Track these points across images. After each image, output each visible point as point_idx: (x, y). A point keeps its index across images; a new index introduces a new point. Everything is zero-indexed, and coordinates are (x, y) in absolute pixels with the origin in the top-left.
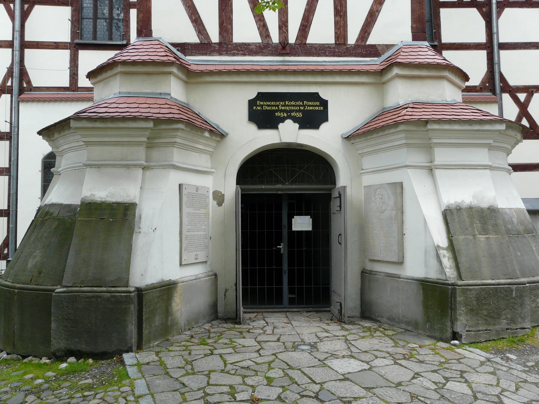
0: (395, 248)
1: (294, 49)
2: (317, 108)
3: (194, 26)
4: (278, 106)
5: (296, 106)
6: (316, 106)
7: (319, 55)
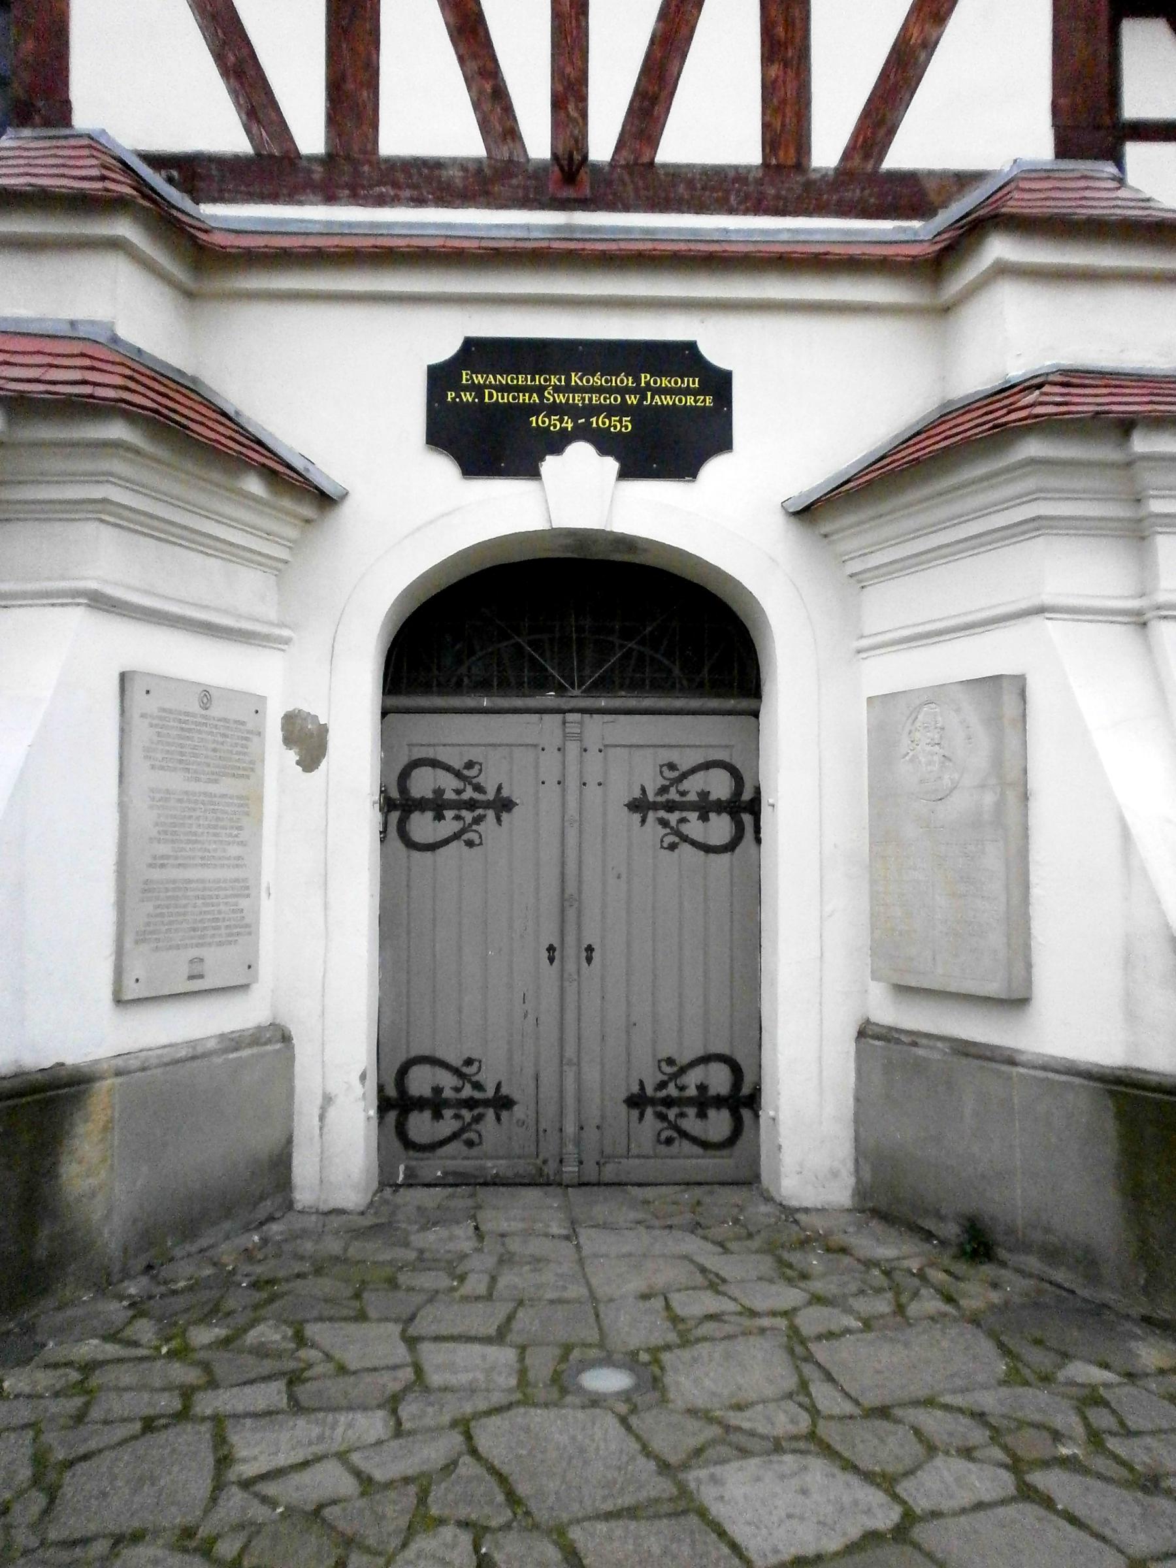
0: (996, 939)
1: (609, 183)
2: (690, 401)
3: (234, 93)
4: (540, 390)
5: (610, 391)
6: (688, 391)
7: (700, 207)
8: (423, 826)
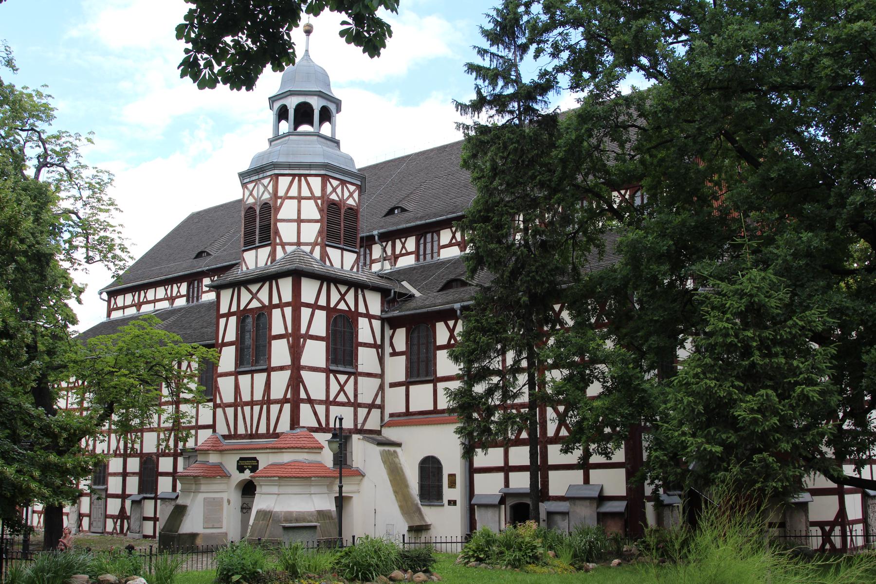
8: (245, 511)
